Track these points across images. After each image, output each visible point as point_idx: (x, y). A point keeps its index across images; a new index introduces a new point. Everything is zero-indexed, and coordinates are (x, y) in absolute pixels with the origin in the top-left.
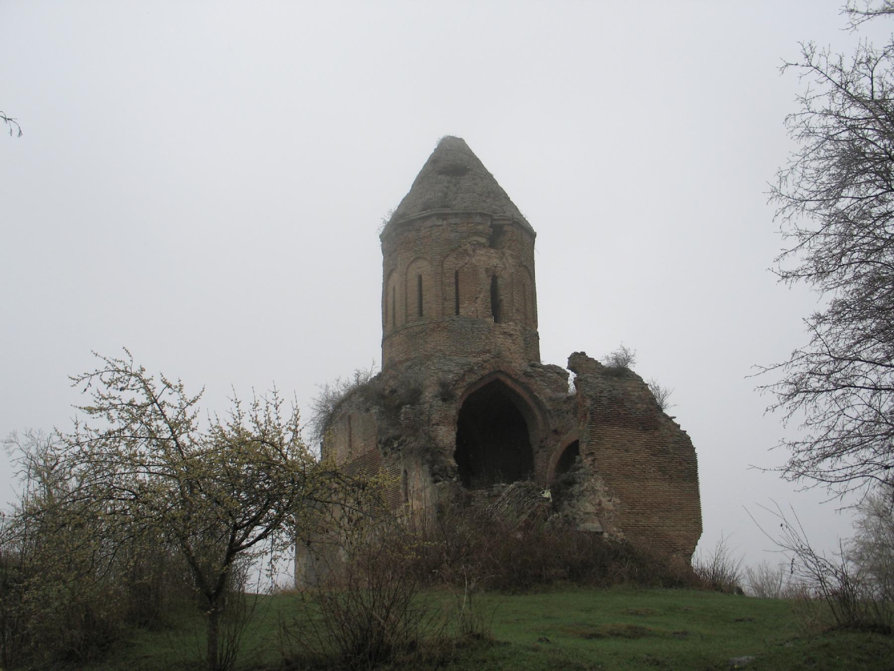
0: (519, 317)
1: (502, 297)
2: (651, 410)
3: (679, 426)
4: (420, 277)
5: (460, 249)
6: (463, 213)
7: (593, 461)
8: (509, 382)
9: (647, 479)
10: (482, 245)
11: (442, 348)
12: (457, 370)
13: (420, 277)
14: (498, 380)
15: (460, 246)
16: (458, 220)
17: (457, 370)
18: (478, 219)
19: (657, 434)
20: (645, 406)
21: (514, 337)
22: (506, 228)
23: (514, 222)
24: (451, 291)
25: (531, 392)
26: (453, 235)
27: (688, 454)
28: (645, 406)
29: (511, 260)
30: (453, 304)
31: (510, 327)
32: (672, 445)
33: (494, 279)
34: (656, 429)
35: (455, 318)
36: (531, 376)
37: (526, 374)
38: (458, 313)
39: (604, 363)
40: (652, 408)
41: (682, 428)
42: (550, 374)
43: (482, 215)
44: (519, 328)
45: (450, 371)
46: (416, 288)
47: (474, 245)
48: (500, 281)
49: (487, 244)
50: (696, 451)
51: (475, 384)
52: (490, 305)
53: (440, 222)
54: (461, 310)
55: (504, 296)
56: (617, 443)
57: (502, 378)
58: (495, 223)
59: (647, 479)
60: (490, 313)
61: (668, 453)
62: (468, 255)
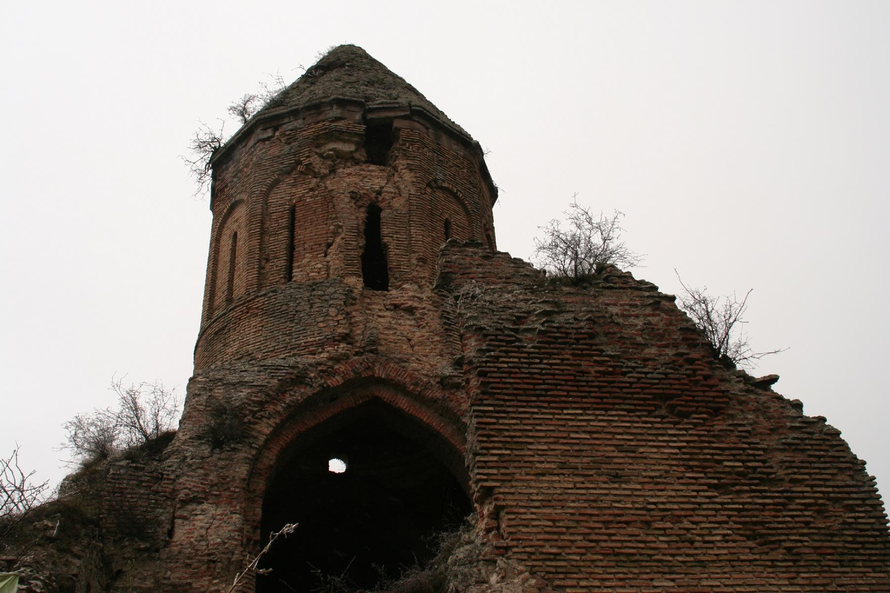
0: (426, 275)
1: (386, 240)
2: (691, 361)
3: (798, 405)
6: (307, 108)
7: (495, 516)
8: (403, 403)
9: (702, 564)
11: (250, 348)
13: (235, 235)
14: (377, 401)
15: (299, 163)
16: (298, 123)
17: (262, 379)
19: (719, 425)
20: (670, 352)
22: (397, 124)
23: (414, 112)
24: (278, 242)
27: (843, 479)
28: (670, 352)
29: (408, 176)
31: (404, 293)
32: (780, 456)
34: (716, 412)
38: (289, 277)
39: (540, 261)
40: (694, 355)
41: (809, 411)
43: (341, 103)
45: (242, 384)
46: (228, 259)
47: (328, 157)
49: (361, 155)
50: (870, 471)
51: (309, 404)
53: (269, 133)
54: (296, 272)
56: (578, 454)
57: (386, 394)
58: (370, 116)
59: (702, 564)
61: (768, 479)
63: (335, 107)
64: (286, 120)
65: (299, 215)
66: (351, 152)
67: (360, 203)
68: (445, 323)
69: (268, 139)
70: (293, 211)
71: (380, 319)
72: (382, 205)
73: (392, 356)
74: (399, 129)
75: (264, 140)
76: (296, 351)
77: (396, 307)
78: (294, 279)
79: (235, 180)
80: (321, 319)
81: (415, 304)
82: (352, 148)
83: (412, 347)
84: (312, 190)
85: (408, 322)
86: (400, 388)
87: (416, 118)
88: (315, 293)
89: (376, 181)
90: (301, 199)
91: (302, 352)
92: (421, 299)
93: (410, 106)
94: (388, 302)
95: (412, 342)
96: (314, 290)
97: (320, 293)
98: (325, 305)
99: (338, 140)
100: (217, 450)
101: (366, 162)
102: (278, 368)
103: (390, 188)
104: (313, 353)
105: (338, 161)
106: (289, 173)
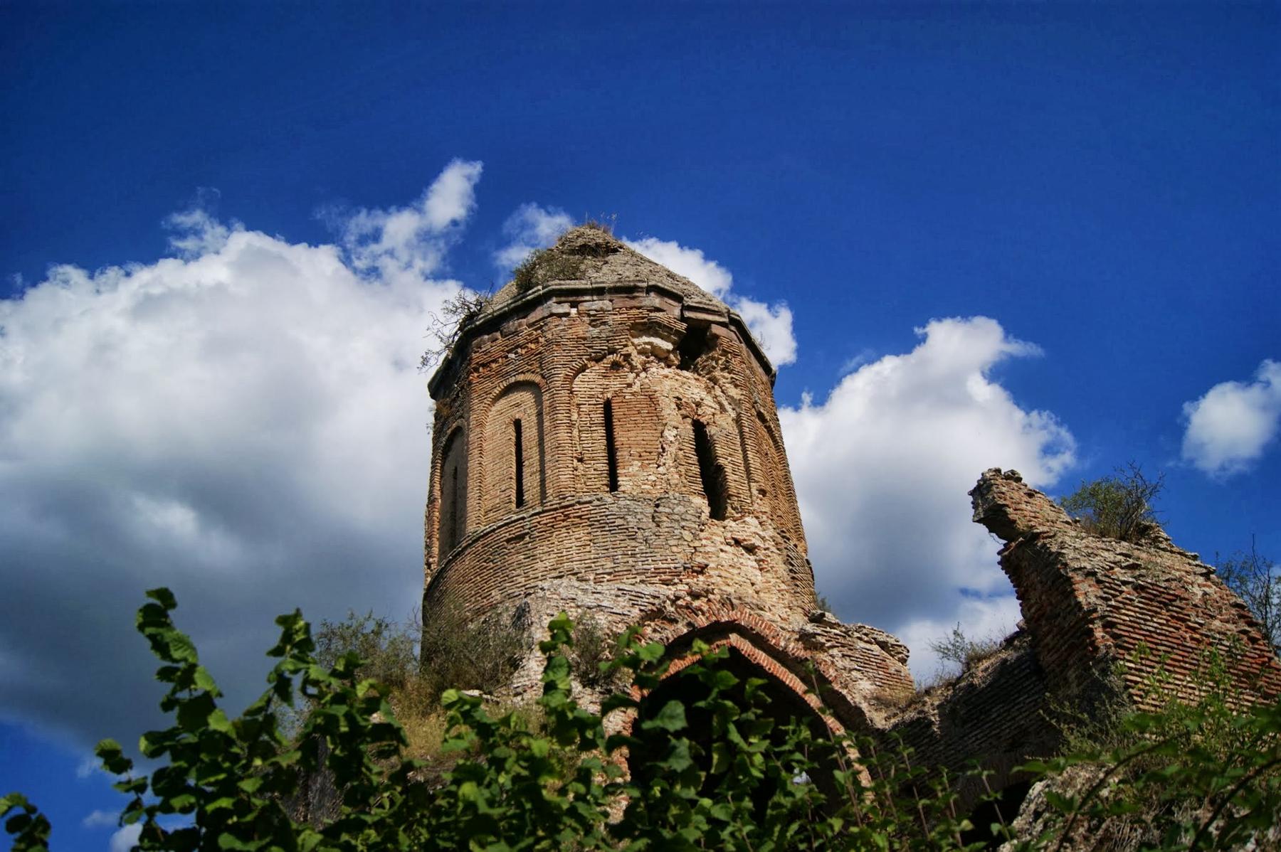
0: (767, 510)
1: (721, 461)
4: (518, 424)
5: (611, 358)
6: (616, 290)
10: (663, 358)
11: (575, 566)
12: (622, 604)
13: (518, 424)
14: (734, 650)
16: (605, 304)
17: (622, 604)
18: (655, 300)
21: (761, 554)
22: (716, 329)
25: (818, 682)
26: (595, 332)
29: (734, 392)
30: (603, 466)
33: (699, 427)
35: (608, 498)
36: (820, 647)
37: (805, 638)
38: (613, 486)
42: (862, 645)
44: (770, 532)
48: (711, 430)
49: (675, 359)
52: (696, 469)
53: (565, 308)
55: (728, 457)
57: (746, 647)
58: (687, 314)
60: (700, 487)
62: (632, 368)
63: (652, 294)
64: (587, 298)
65: (617, 413)
66: (668, 351)
67: (683, 412)
68: (791, 571)
69: (567, 315)
70: (608, 406)
71: (722, 554)
72: (703, 420)
73: (747, 600)
74: (717, 337)
75: (560, 316)
76: (643, 577)
77: (737, 542)
78: (622, 488)
79: (512, 356)
80: (675, 542)
81: (758, 542)
82: (670, 346)
83: (757, 592)
84: (629, 385)
85: (750, 563)
86: (759, 641)
87: (733, 328)
88: (660, 509)
89: (696, 391)
90: (616, 394)
91: (653, 580)
92: (763, 538)
93: (729, 312)
94: (729, 535)
95: (757, 587)
96: (657, 506)
97: (667, 510)
98: (676, 525)
99: (656, 335)
100: (589, 690)
101: (678, 367)
102: (639, 595)
103: (709, 400)
104: (665, 583)
105: (652, 358)
106: (598, 360)
